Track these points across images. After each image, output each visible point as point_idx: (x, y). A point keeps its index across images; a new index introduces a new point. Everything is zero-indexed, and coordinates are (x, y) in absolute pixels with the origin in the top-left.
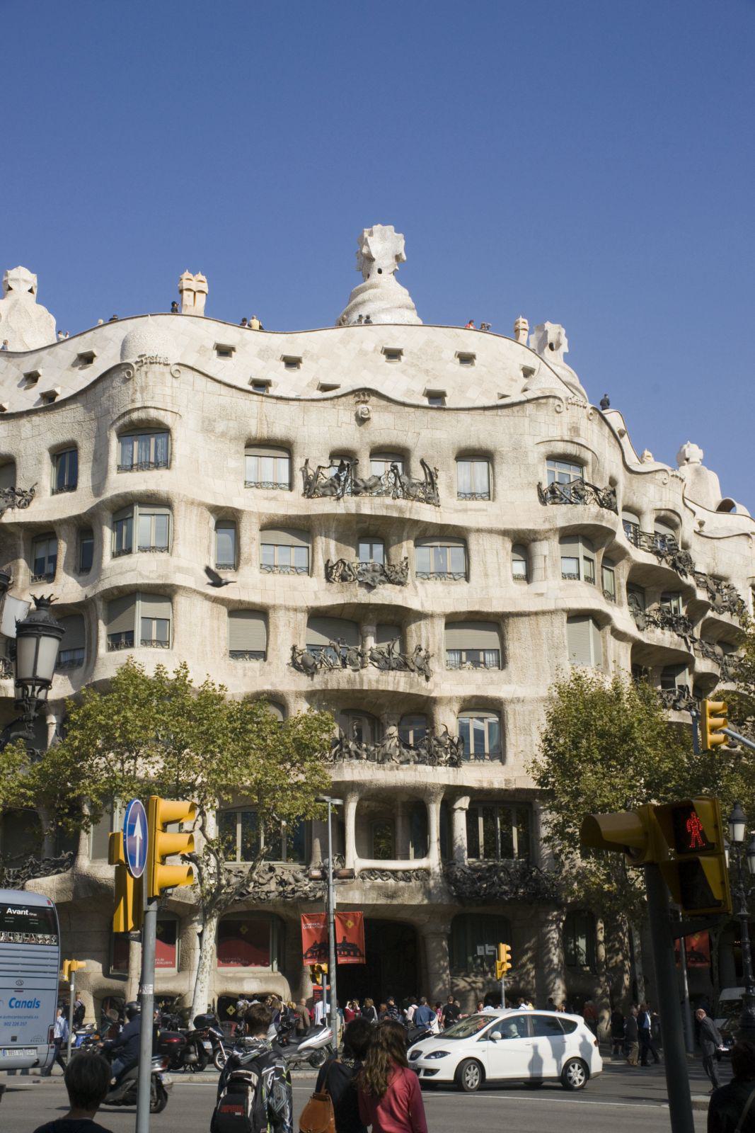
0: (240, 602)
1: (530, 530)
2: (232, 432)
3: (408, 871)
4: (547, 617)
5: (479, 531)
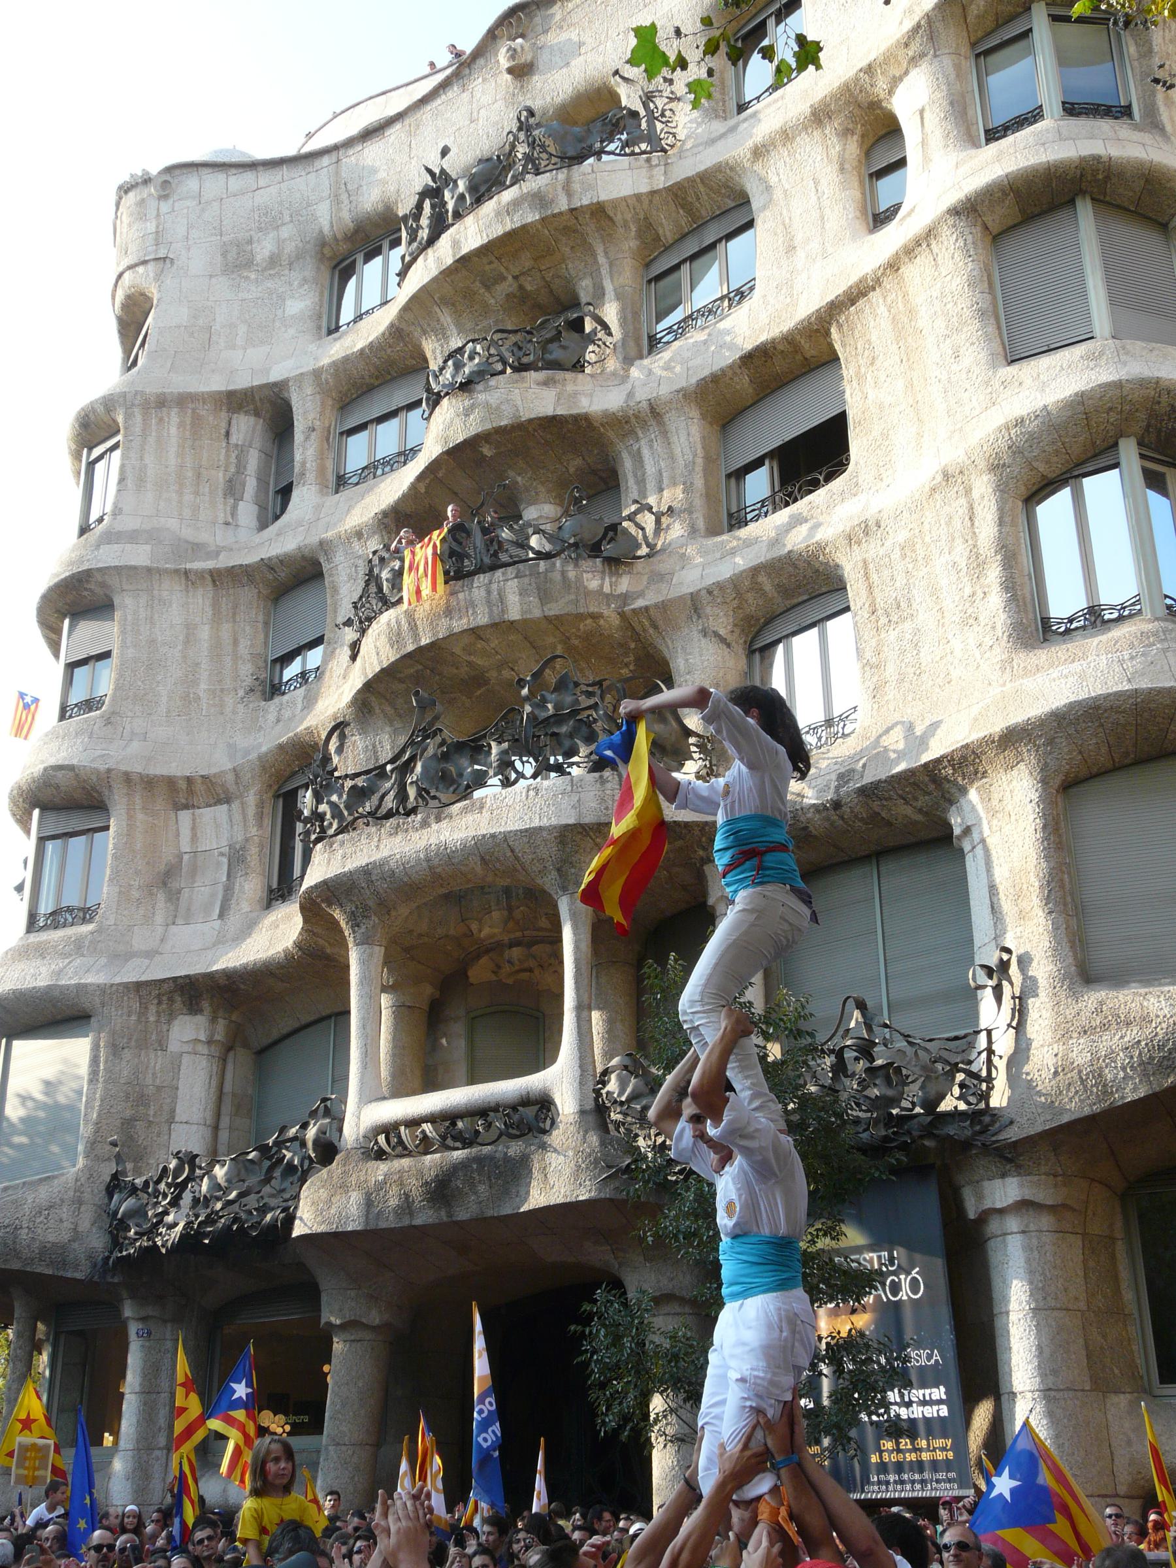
0: (268, 565)
1: (869, 70)
2: (289, 248)
3: (482, 1112)
4: (923, 260)
5: (759, 152)
